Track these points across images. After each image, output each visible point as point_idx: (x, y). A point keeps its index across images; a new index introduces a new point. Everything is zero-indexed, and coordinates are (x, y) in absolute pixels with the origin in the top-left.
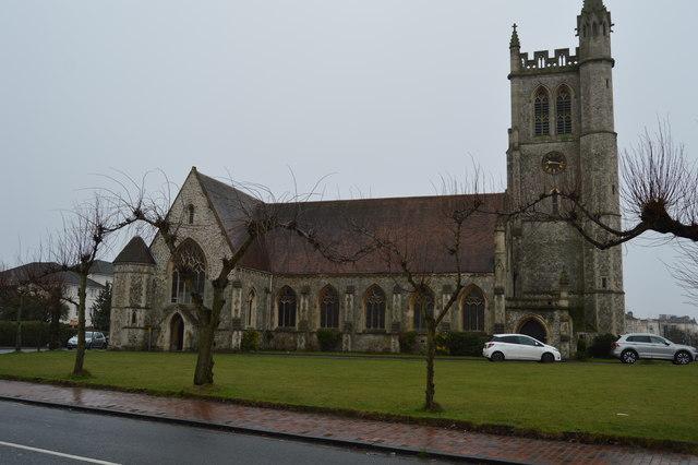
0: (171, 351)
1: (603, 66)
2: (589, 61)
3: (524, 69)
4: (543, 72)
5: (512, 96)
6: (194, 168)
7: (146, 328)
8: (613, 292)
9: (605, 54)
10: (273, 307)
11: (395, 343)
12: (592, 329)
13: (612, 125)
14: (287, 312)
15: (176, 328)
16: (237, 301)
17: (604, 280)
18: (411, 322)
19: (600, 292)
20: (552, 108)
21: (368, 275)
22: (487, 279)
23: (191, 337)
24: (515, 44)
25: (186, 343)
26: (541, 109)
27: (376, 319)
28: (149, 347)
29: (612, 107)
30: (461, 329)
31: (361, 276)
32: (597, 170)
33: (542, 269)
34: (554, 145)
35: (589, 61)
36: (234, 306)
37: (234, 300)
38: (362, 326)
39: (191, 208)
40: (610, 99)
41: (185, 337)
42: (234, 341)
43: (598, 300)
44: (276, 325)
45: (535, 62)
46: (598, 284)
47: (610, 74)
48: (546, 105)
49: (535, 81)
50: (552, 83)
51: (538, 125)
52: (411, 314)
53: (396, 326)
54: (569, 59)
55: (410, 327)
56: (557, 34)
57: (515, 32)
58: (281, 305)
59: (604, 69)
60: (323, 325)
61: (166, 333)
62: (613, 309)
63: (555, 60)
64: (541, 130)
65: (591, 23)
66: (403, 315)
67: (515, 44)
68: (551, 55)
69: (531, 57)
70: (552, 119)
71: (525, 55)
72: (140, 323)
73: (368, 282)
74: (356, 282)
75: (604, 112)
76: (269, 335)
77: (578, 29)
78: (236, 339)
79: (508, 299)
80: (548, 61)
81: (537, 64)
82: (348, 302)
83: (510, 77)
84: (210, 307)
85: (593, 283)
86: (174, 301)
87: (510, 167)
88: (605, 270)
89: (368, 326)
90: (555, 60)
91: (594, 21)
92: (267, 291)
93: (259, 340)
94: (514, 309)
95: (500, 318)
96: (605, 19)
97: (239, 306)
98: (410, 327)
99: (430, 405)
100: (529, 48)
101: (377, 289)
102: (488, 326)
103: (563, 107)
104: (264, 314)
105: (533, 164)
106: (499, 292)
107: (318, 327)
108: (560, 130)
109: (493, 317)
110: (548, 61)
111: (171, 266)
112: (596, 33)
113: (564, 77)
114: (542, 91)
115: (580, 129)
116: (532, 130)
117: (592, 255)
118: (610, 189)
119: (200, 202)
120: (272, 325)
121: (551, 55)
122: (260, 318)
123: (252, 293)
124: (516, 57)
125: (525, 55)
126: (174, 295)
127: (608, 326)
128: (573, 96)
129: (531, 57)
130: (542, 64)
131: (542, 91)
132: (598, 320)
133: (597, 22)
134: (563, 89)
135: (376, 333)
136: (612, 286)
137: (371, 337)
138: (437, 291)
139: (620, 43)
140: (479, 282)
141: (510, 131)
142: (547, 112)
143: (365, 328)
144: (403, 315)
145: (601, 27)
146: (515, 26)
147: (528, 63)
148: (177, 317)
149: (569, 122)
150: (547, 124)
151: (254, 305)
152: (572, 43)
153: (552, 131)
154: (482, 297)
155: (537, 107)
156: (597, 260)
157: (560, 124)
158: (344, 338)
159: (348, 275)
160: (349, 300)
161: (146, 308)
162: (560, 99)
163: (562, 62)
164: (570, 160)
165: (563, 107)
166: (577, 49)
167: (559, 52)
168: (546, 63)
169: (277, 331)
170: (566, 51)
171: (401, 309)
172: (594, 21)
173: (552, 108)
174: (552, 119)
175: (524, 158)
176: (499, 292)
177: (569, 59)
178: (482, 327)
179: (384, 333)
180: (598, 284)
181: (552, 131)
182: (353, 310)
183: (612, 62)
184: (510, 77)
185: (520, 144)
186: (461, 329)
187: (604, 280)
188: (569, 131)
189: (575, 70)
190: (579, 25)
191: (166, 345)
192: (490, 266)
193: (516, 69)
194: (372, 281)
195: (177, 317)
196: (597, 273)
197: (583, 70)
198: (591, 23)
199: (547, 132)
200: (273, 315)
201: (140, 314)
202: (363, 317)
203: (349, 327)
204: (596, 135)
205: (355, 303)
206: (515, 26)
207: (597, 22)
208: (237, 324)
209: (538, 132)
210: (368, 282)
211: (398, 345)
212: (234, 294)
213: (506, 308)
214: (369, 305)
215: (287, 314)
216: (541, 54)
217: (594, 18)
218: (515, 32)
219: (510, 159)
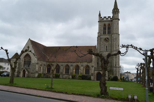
0: (23, 77)
1: (117, 20)
2: (114, 19)
3: (101, 20)
4: (105, 21)
5: (99, 26)
6: (30, 39)
7: (17, 72)
8: (117, 67)
9: (117, 18)
10: (46, 69)
11: (71, 77)
12: (113, 74)
13: (118, 32)
14: (49, 69)
15: (24, 72)
16: (37, 67)
17: (116, 64)
18: (74, 73)
19: (115, 67)
21: (66, 62)
22: (90, 64)
23: (27, 75)
24: (100, 15)
25: (26, 76)
26: (105, 29)
27: (67, 72)
28: (18, 76)
29: (119, 29)
30: (84, 74)
31: (65, 62)
32: (115, 42)
34: (107, 36)
35: (114, 19)
36: (36, 68)
37: (36, 67)
38: (64, 73)
39: (28, 47)
40: (118, 27)
41: (26, 74)
42: (36, 76)
43: (114, 69)
44: (46, 72)
45: (104, 19)
46: (115, 65)
47: (118, 22)
50: (107, 23)
52: (74, 71)
53: (71, 73)
54: (111, 18)
55: (74, 74)
56: (108, 13)
57: (100, 12)
58: (48, 68)
59: (117, 21)
60: (56, 72)
61: (22, 73)
62: (117, 70)
63: (108, 19)
64: (104, 33)
65: (115, 11)
66: (73, 71)
67: (100, 15)
68: (107, 18)
69: (103, 18)
70: (107, 31)
71: (102, 17)
73: (66, 64)
74: (63, 64)
75: (117, 30)
76: (45, 74)
77: (112, 12)
78: (36, 75)
79: (94, 68)
80: (106, 19)
81: (104, 19)
82: (62, 68)
83: (98, 22)
84: (14, 67)
85: (113, 65)
86: (24, 67)
87: (98, 40)
88: (116, 62)
89: (66, 73)
90: (108, 19)
91: (116, 10)
92: (45, 65)
93: (42, 75)
94: (96, 70)
95: (93, 72)
96: (118, 11)
97: (38, 68)
98: (74, 74)
99: (52, 88)
100: (102, 16)
101: (68, 65)
102: (90, 74)
103: (109, 28)
104: (44, 70)
105: (102, 40)
106: (92, 67)
107: (55, 73)
108: (108, 33)
109: (91, 72)
110: (106, 19)
111: (24, 59)
112: (116, 13)
113: (110, 22)
114: (105, 25)
115: (112, 33)
116: (102, 33)
117: (113, 59)
118: (118, 46)
119: (31, 46)
120: (46, 72)
121: (107, 18)
122: (43, 71)
123: (41, 65)
124: (100, 18)
125: (102, 17)
126: (24, 65)
127: (116, 74)
128: (111, 26)
129: (103, 18)
130: (105, 19)
131: (105, 25)
132: (114, 73)
133: (116, 11)
134: (109, 25)
135: (67, 75)
136: (117, 66)
137: (66, 75)
138: (80, 66)
139: (120, 16)
140: (89, 64)
141: (98, 33)
142: (106, 29)
143: (65, 73)
144: (73, 71)
145: (117, 13)
146: (100, 11)
148: (24, 70)
149: (110, 31)
151: (41, 68)
152: (111, 15)
154: (89, 68)
155: (104, 28)
156: (114, 60)
157: (108, 32)
158: (60, 75)
159: (62, 62)
160: (62, 67)
161: (18, 68)
162: (108, 27)
163: (109, 19)
164: (110, 40)
165: (109, 28)
166: (112, 16)
167: (109, 17)
169: (46, 74)
170: (109, 17)
171: (72, 70)
172: (116, 10)
173: (107, 28)
174: (107, 31)
175: (101, 39)
176: (92, 67)
177: (111, 18)
178: (89, 74)
179: (69, 75)
180: (115, 65)
181: (107, 33)
182: (62, 69)
183: (119, 20)
184: (98, 22)
185: (100, 36)
186: (84, 74)
187: (116, 64)
188: (110, 33)
189: (112, 21)
190: (113, 11)
191: (22, 76)
192: (91, 61)
193: (100, 20)
194: (67, 63)
195: (24, 70)
196: (114, 63)
197: (113, 21)
198: (115, 11)
199: (106, 34)
200: (46, 70)
202: (65, 71)
203: (62, 73)
204: (115, 34)
205: (63, 68)
206: (100, 11)
207: (116, 11)
208: (37, 72)
209: (104, 33)
210: (66, 64)
211: (71, 77)
212: (37, 65)
213: (94, 70)
214: (66, 69)
215: (49, 70)
216: (105, 17)
217: (116, 10)
218: (100, 12)
219: (98, 39)
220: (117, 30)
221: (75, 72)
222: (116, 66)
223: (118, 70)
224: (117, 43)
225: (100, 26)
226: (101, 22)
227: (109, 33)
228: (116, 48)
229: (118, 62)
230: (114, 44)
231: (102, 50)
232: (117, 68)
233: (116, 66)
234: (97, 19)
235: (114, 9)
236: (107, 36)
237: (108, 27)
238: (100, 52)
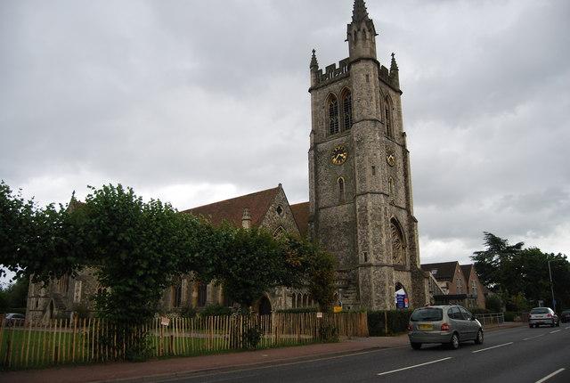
3: (322, 80)
8: (370, 265)
18: (194, 303)
24: (314, 64)
26: (333, 113)
33: (333, 249)
43: (361, 273)
46: (361, 258)
49: (326, 90)
50: (336, 88)
52: (195, 294)
56: (335, 50)
57: (314, 56)
64: (333, 129)
67: (314, 64)
68: (337, 67)
70: (339, 118)
72: (40, 307)
91: (361, 28)
96: (364, 25)
97: (80, 293)
100: (322, 66)
103: (348, 106)
114: (332, 97)
116: (324, 130)
118: (369, 171)
121: (337, 67)
130: (332, 75)
146: (314, 51)
155: (331, 110)
156: (359, 237)
161: (46, 297)
162: (353, 101)
172: (361, 28)
174: (339, 118)
187: (365, 254)
190: (349, 34)
201: (41, 301)
206: (314, 51)
209: (332, 132)
216: (334, 65)
217: (355, 28)
218: (314, 56)
219: (309, 155)
220: (364, 103)
221: (198, 299)
222: (366, 261)
223: (373, 277)
224: (366, 158)
225: (315, 104)
226: (317, 89)
227: (348, 123)
228: (363, 180)
229: (375, 243)
230: (357, 164)
231: (323, 203)
232: (372, 269)
233: (366, 261)
234: (307, 81)
235: (349, 26)
236: (337, 141)
237: (353, 101)
238: (318, 210)
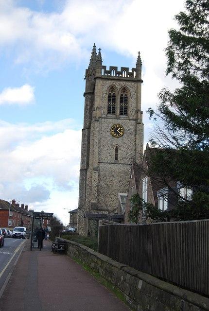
20: (118, 101)
26: (111, 99)
45: (110, 72)
48: (114, 97)
49: (110, 83)
51: (109, 108)
54: (128, 73)
64: (111, 110)
68: (119, 70)
69: (108, 69)
71: (105, 67)
80: (117, 73)
81: (110, 73)
100: (107, 63)
103: (124, 100)
108: (121, 113)
110: (117, 73)
114: (112, 88)
121: (119, 70)
129: (108, 69)
130: (113, 74)
134: (124, 89)
142: (114, 101)
147: (106, 72)
150: (114, 108)
153: (118, 111)
155: (109, 97)
157: (121, 108)
168: (116, 74)
170: (125, 69)
173: (118, 101)
185: (100, 117)
199: (114, 113)
209: (109, 112)
216: (114, 68)
227: (124, 111)
238: (99, 163)
